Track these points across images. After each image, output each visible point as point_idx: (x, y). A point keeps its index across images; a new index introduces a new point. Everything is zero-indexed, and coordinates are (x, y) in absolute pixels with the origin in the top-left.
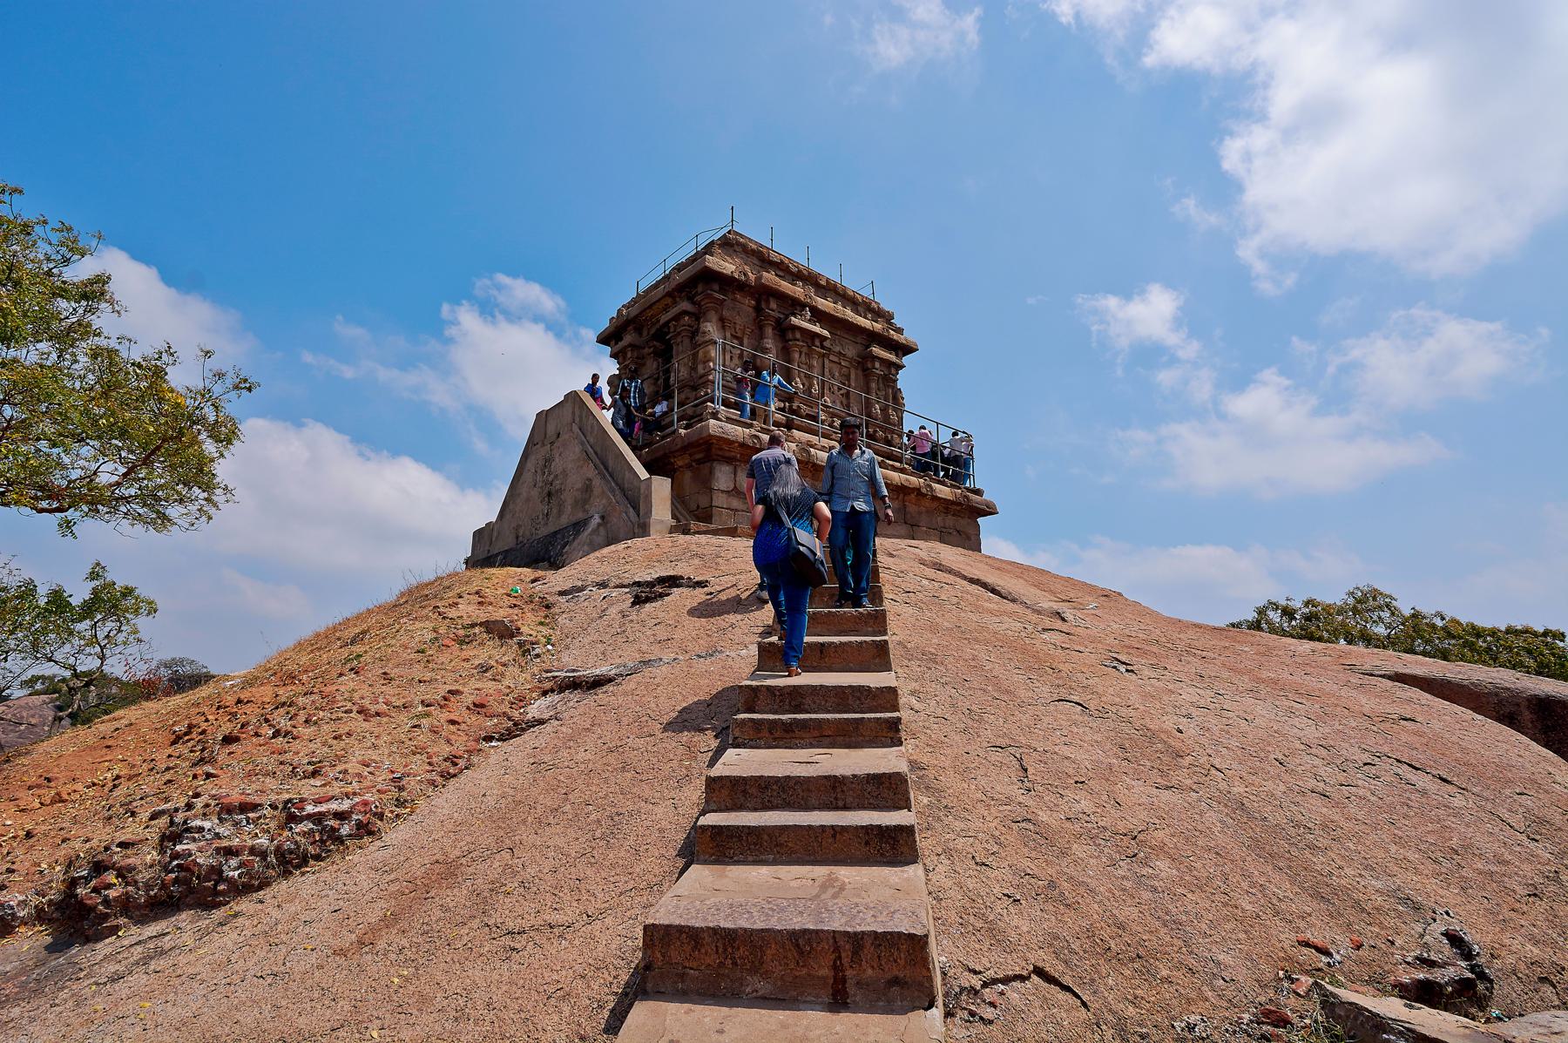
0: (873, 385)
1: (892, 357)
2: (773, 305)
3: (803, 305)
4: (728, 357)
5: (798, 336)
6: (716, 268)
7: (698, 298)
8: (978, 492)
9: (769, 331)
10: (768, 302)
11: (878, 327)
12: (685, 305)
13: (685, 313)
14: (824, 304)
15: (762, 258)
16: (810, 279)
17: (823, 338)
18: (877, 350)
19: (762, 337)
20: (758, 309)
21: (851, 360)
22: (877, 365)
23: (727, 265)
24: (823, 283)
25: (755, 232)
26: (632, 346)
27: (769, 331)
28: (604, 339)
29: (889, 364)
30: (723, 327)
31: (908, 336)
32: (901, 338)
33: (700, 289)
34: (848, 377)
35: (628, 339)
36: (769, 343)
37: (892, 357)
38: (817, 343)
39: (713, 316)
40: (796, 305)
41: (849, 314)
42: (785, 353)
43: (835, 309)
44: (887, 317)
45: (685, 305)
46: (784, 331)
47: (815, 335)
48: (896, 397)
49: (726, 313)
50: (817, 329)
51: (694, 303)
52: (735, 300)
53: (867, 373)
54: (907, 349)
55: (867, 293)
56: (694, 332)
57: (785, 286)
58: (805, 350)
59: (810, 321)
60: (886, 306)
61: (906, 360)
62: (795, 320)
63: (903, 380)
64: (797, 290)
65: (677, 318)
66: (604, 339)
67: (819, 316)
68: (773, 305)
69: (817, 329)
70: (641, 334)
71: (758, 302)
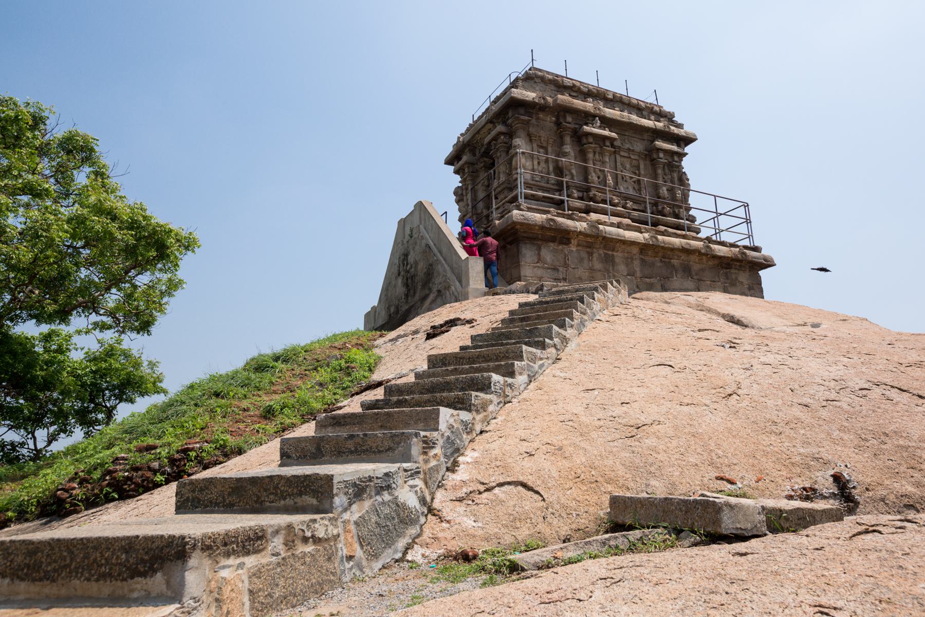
0: (660, 171)
1: (674, 148)
2: (569, 119)
4: (536, 162)
5: (591, 140)
6: (520, 97)
7: (510, 121)
8: (756, 249)
9: (568, 139)
10: (565, 117)
11: (660, 125)
12: (500, 128)
13: (500, 133)
15: (558, 84)
18: (659, 144)
19: (562, 144)
20: (558, 124)
21: (639, 154)
22: (661, 155)
24: (610, 96)
25: (551, 65)
27: (568, 139)
28: (449, 162)
29: (672, 153)
30: (531, 140)
31: (689, 129)
32: (681, 132)
33: (510, 114)
34: (638, 168)
35: (465, 158)
36: (568, 148)
38: (608, 143)
39: (521, 133)
41: (635, 118)
42: (582, 154)
43: (622, 117)
44: (669, 117)
45: (500, 128)
46: (580, 138)
47: (605, 138)
48: (682, 180)
50: (606, 133)
51: (507, 125)
52: (538, 119)
53: (653, 162)
54: (688, 140)
55: (651, 100)
56: (509, 147)
57: (578, 103)
58: (598, 149)
59: (600, 127)
60: (667, 108)
63: (687, 165)
64: (588, 105)
65: (495, 139)
66: (449, 162)
67: (607, 122)
68: (569, 119)
69: (606, 133)
70: (474, 155)
71: (558, 118)
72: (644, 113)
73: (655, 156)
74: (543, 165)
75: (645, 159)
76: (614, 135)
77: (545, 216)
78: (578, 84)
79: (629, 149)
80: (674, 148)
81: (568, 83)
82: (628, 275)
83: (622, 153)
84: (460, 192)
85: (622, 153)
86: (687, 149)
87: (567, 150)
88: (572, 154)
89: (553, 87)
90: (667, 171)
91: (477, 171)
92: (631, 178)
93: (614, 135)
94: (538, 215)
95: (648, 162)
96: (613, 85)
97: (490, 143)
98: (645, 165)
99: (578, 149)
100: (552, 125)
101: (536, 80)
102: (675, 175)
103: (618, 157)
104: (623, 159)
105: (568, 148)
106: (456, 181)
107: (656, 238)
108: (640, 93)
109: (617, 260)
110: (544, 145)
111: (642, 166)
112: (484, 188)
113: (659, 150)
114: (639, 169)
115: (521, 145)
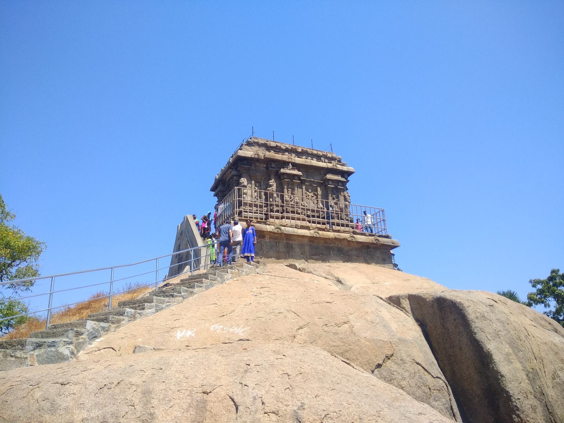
1: (339, 178)
2: (273, 165)
3: (288, 163)
5: (286, 177)
6: (243, 155)
10: (271, 164)
11: (330, 165)
12: (234, 172)
13: (234, 176)
14: (298, 160)
17: (298, 177)
18: (329, 176)
20: (267, 168)
23: (248, 152)
28: (212, 190)
32: (345, 168)
37: (339, 178)
40: (285, 164)
41: (315, 162)
43: (306, 162)
45: (234, 172)
46: (280, 177)
47: (294, 176)
50: (296, 172)
51: (238, 171)
52: (256, 166)
62: (282, 170)
64: (285, 157)
65: (231, 178)
66: (212, 190)
67: (296, 166)
68: (273, 165)
69: (296, 172)
70: (224, 186)
71: (267, 165)
76: (300, 173)
86: (349, 178)
90: (335, 192)
92: (312, 197)
93: (300, 173)
100: (264, 169)
109: (294, 246)
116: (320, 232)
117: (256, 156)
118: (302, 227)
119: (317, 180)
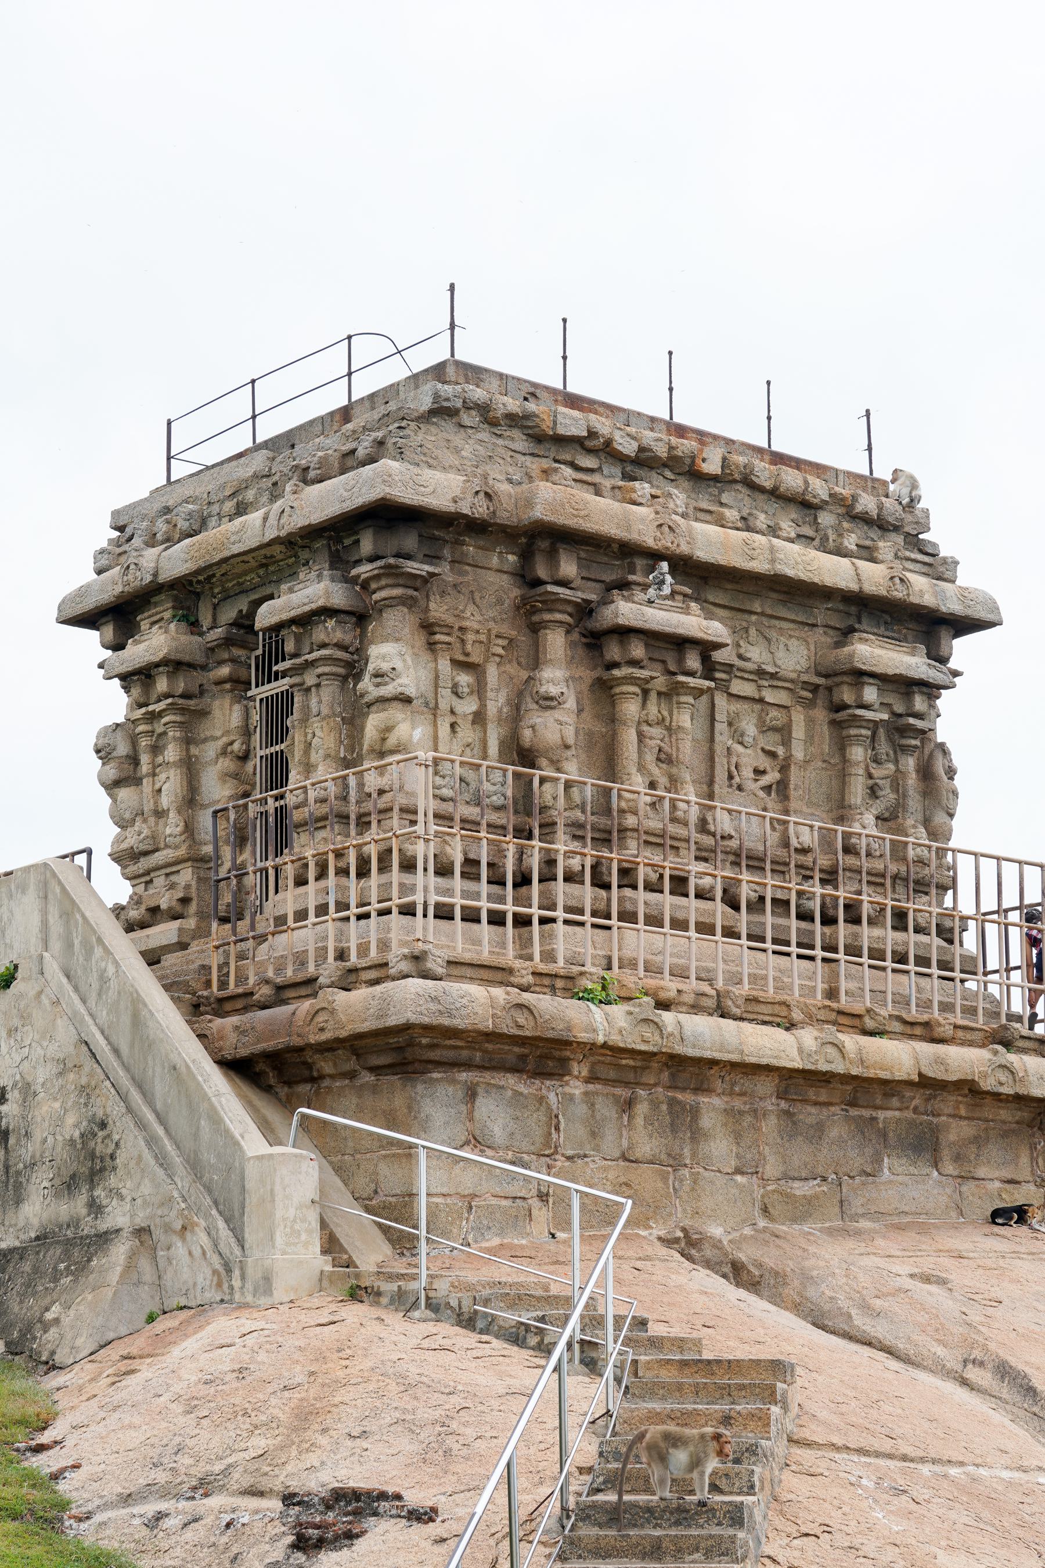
2: (568, 568)
4: (444, 730)
7: (364, 570)
9: (556, 642)
14: (712, 541)
16: (673, 460)
17: (706, 648)
19: (536, 662)
21: (793, 685)
22: (870, 694)
23: (435, 481)
24: (712, 466)
25: (514, 350)
26: (175, 665)
27: (556, 642)
29: (907, 685)
31: (976, 576)
33: (367, 544)
34: (784, 732)
35: (155, 641)
36: (554, 678)
38: (693, 662)
39: (397, 620)
40: (622, 559)
42: (604, 692)
47: (680, 643)
49: (438, 609)
53: (841, 720)
56: (352, 668)
58: (660, 682)
61: (963, 650)
65: (305, 621)
69: (692, 622)
70: (194, 626)
71: (526, 556)
72: (826, 519)
73: (847, 696)
74: (467, 733)
75: (810, 704)
76: (715, 629)
77: (498, 992)
78: (603, 426)
79: (761, 673)
80: (911, 662)
81: (572, 423)
82: (738, 1171)
83: (738, 687)
84: (123, 749)
85: (738, 687)
87: (554, 690)
88: (571, 703)
89: (521, 443)
90: (884, 748)
91: (202, 691)
92: (759, 772)
94: (476, 990)
95: (821, 714)
96: (722, 410)
97: (277, 628)
98: (810, 722)
99: (589, 675)
100: (505, 580)
101: (466, 419)
102: (910, 763)
103: (721, 700)
104: (736, 706)
105: (554, 678)
106: (115, 704)
107: (840, 1048)
108: (821, 437)
109: (706, 1121)
110: (475, 659)
111: (799, 732)
112: (226, 764)
113: (860, 676)
114: (786, 742)
115: (394, 656)
116: (851, 1041)
117: (480, 509)
118: (759, 1010)
119: (793, 654)
